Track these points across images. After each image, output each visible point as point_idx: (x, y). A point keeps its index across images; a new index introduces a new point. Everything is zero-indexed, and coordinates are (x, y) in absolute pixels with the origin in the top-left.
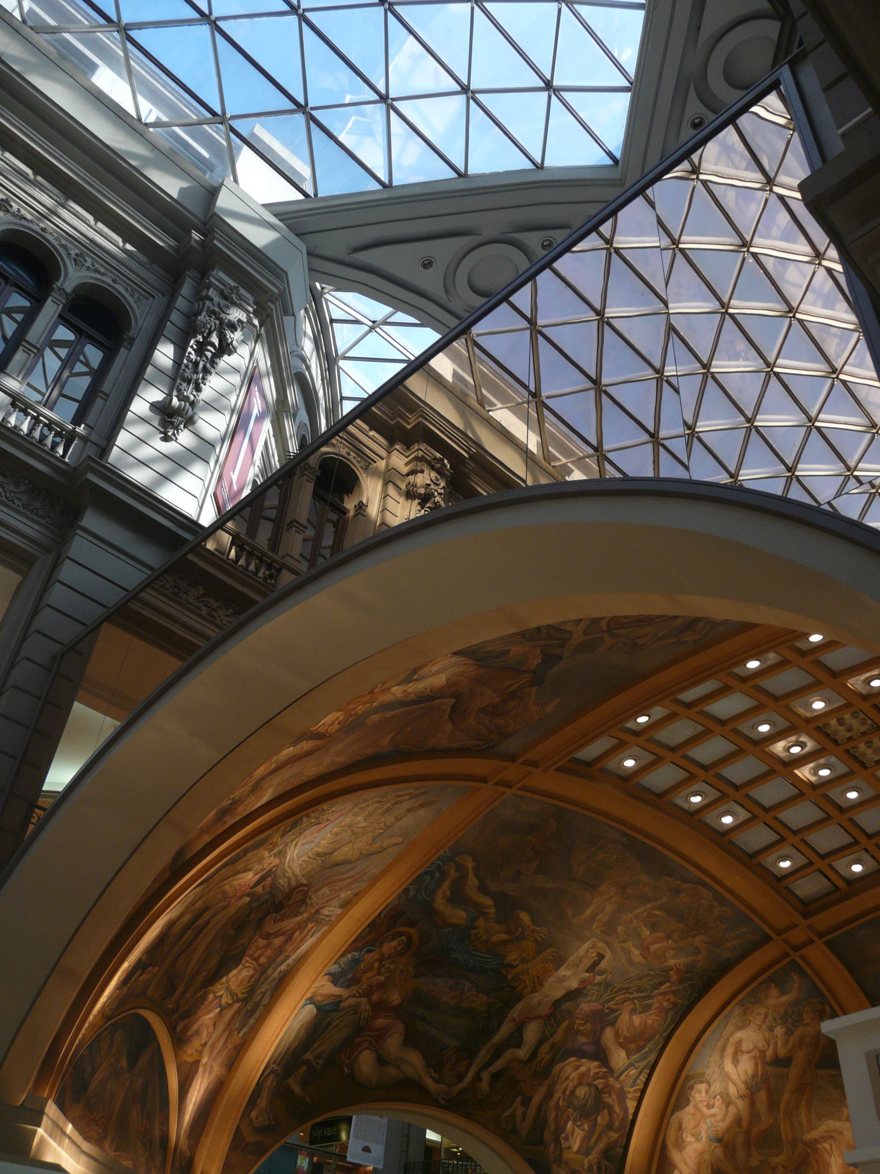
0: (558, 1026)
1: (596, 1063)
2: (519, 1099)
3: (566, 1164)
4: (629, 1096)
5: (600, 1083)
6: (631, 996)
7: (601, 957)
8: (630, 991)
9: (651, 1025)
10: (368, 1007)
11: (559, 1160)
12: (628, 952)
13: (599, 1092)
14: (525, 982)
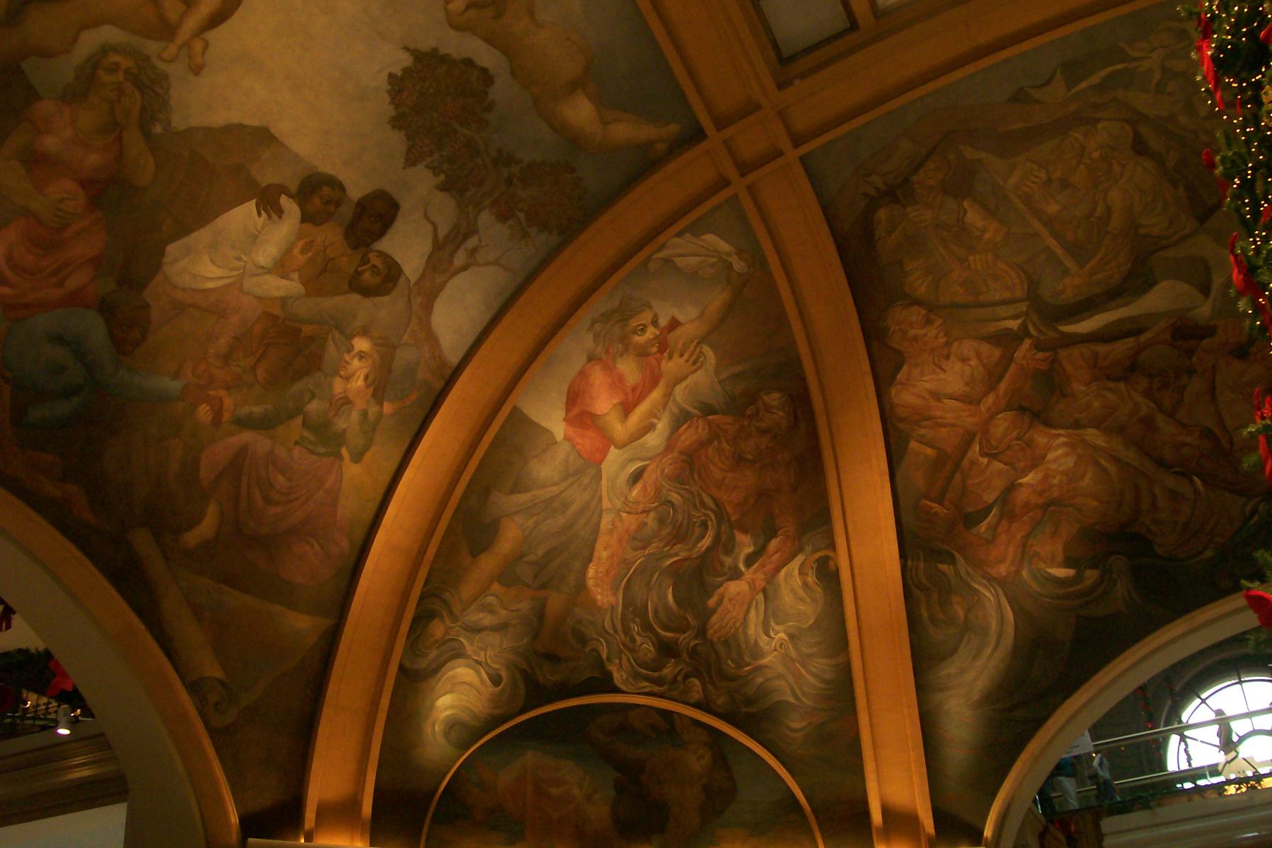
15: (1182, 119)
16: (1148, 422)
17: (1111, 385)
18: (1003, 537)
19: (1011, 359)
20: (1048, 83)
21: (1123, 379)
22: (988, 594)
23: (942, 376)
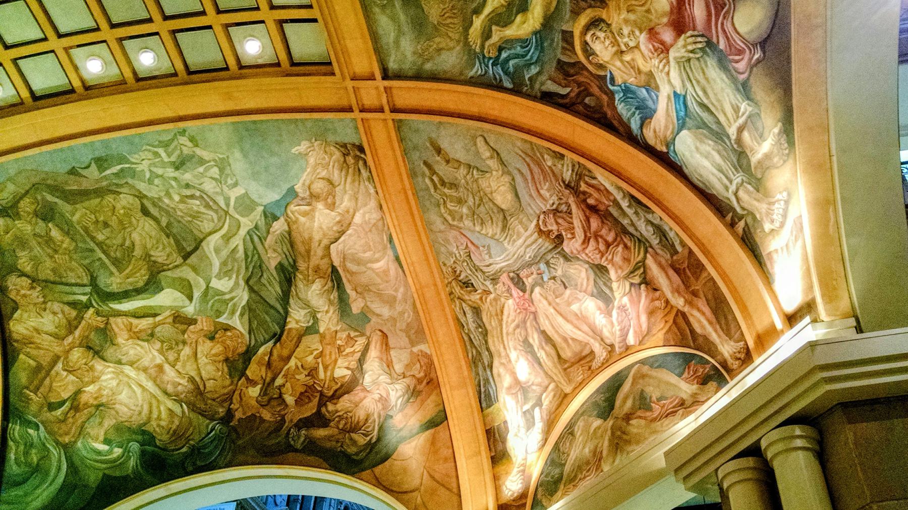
10: (681, 41)
15: (166, 201)
16: (160, 368)
17: (140, 342)
18: (71, 420)
19: (82, 318)
20: (87, 167)
21: (147, 341)
22: (55, 452)
23: (42, 320)
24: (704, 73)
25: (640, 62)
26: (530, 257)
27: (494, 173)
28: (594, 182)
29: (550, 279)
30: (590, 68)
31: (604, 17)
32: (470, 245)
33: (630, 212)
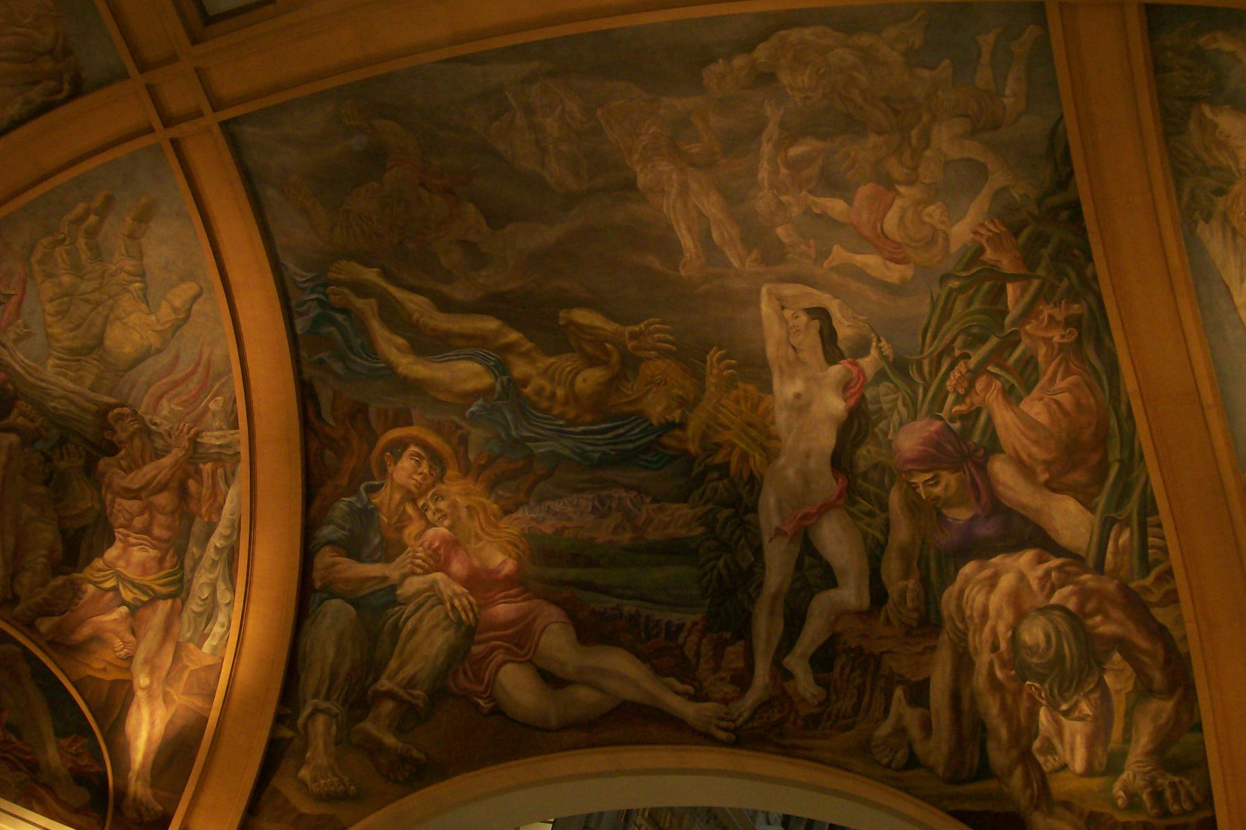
0: (884, 507)
1: (1025, 559)
2: (899, 693)
3: (1067, 805)
4: (1153, 598)
5: (1067, 597)
6: (972, 363)
7: (821, 314)
8: (957, 352)
9: (1078, 404)
10: (459, 589)
11: (1044, 797)
12: (860, 274)
13: (1076, 619)
14: (734, 446)
24: (434, 627)
25: (412, 529)
26: (55, 408)
27: (153, 318)
28: (222, 485)
29: (43, 454)
30: (376, 453)
31: (452, 472)
32: (15, 300)
33: (210, 553)
